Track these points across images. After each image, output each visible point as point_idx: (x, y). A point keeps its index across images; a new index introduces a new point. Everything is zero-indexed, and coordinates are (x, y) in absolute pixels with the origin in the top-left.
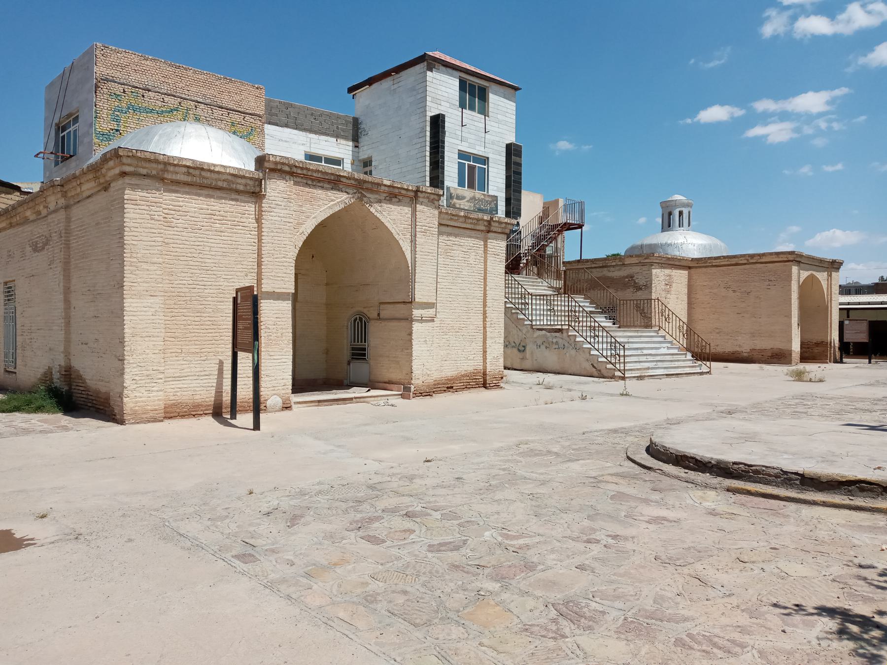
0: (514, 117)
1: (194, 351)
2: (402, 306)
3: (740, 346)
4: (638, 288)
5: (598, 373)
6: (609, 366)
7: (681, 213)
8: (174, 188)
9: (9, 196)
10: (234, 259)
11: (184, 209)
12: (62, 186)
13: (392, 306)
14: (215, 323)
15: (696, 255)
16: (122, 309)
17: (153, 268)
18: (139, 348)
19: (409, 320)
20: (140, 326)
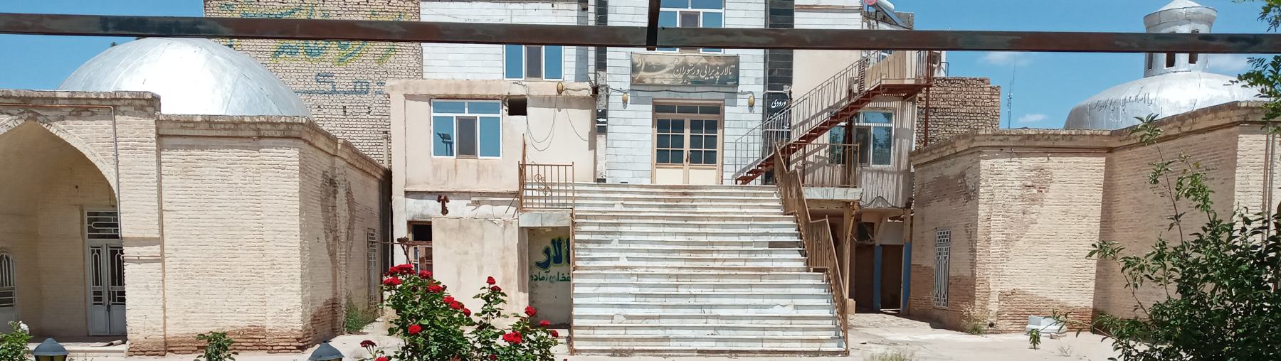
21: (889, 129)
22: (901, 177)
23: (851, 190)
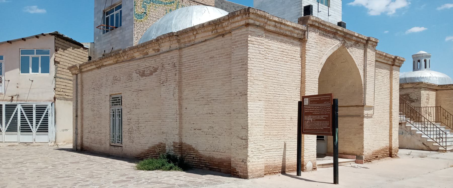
0: (341, 8)
1: (274, 134)
2: (355, 108)
4: (412, 101)
5: (427, 147)
6: (434, 144)
7: (425, 61)
8: (267, 34)
9: (78, 50)
10: (291, 79)
11: (271, 48)
12: (178, 36)
13: (346, 108)
14: (284, 117)
15: (438, 83)
16: (246, 108)
17: (260, 83)
18: (254, 132)
19: (361, 116)
20: (255, 119)
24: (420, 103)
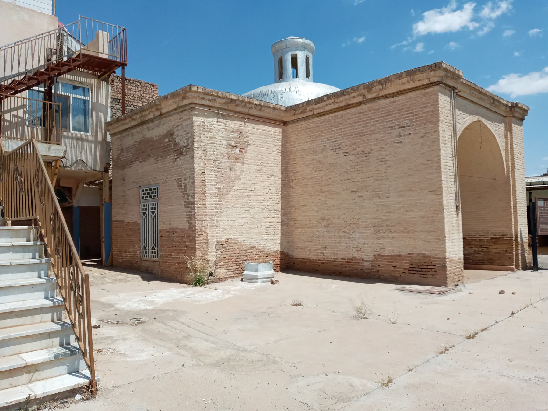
3: (359, 250)
21: (85, 101)
22: (98, 147)
23: (54, 147)
24: (193, 158)
